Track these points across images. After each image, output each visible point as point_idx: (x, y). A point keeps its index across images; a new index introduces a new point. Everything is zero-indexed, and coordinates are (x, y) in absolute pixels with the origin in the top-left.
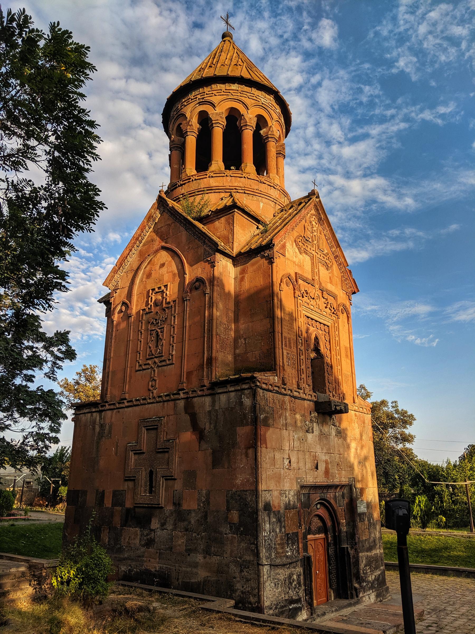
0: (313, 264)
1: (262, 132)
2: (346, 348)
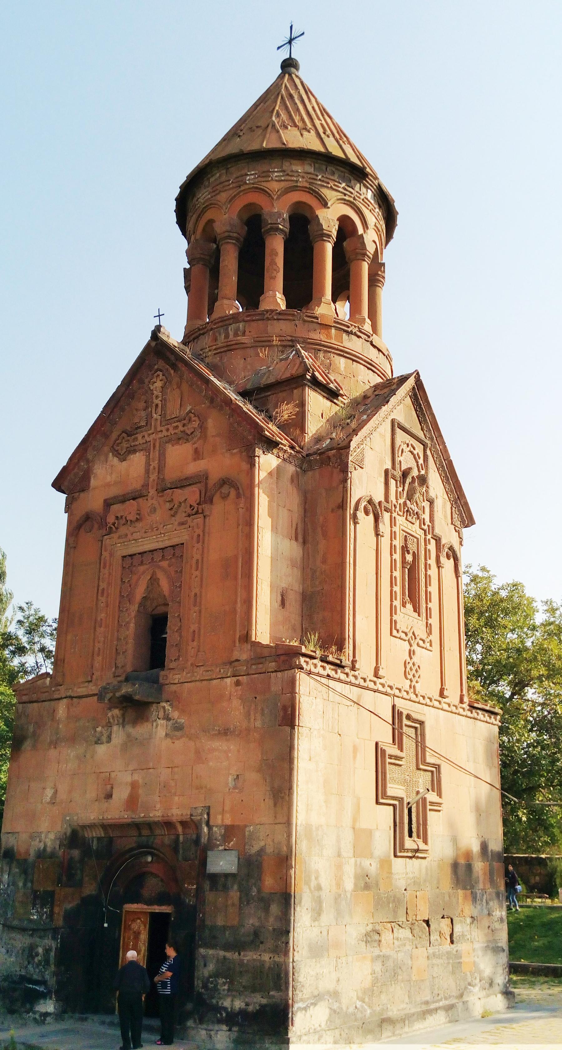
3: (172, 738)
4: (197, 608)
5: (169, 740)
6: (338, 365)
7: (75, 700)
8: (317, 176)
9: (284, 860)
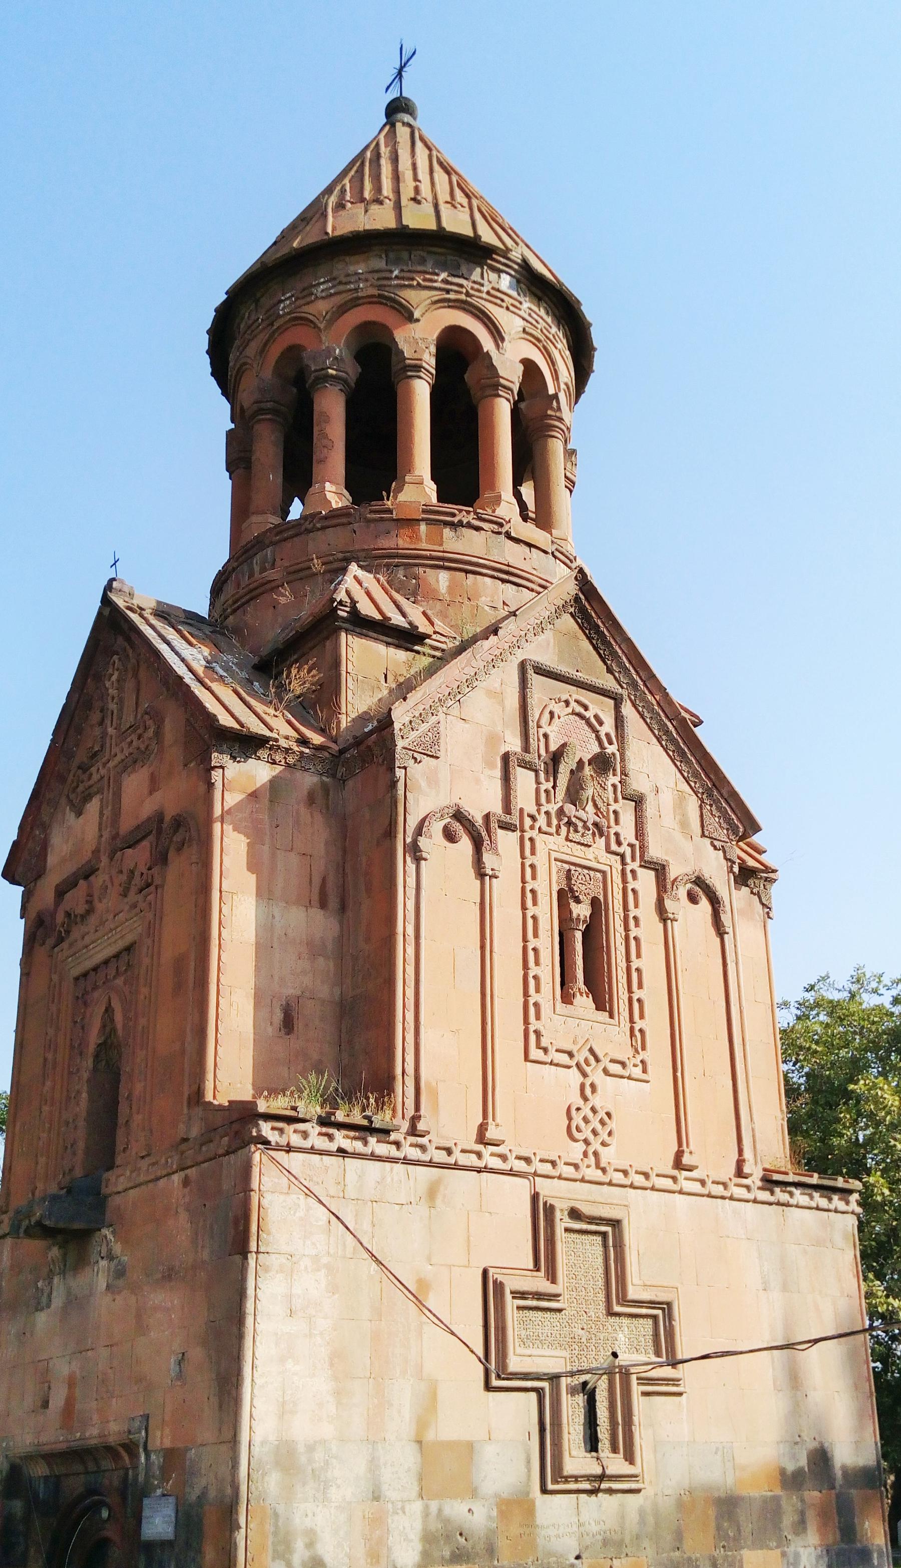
3: (113, 1293)
4: (144, 1052)
6: (434, 585)
8: (391, 272)
9: (228, 1511)
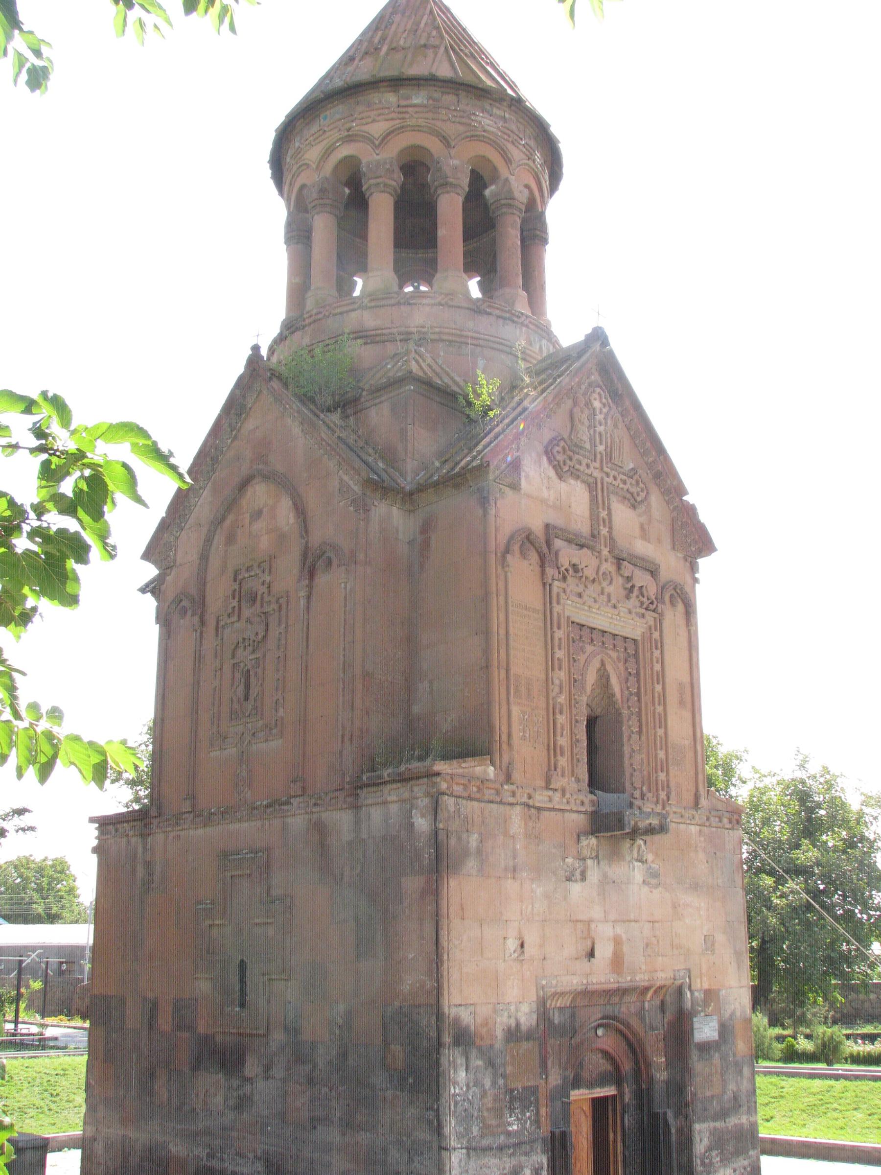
0: (594, 500)
1: (487, 192)
2: (681, 685)
5: (645, 889)
7: (532, 810)
